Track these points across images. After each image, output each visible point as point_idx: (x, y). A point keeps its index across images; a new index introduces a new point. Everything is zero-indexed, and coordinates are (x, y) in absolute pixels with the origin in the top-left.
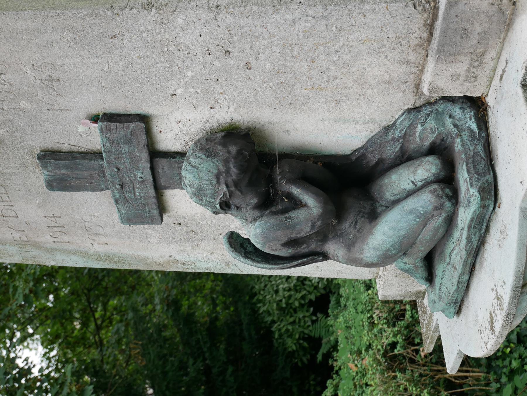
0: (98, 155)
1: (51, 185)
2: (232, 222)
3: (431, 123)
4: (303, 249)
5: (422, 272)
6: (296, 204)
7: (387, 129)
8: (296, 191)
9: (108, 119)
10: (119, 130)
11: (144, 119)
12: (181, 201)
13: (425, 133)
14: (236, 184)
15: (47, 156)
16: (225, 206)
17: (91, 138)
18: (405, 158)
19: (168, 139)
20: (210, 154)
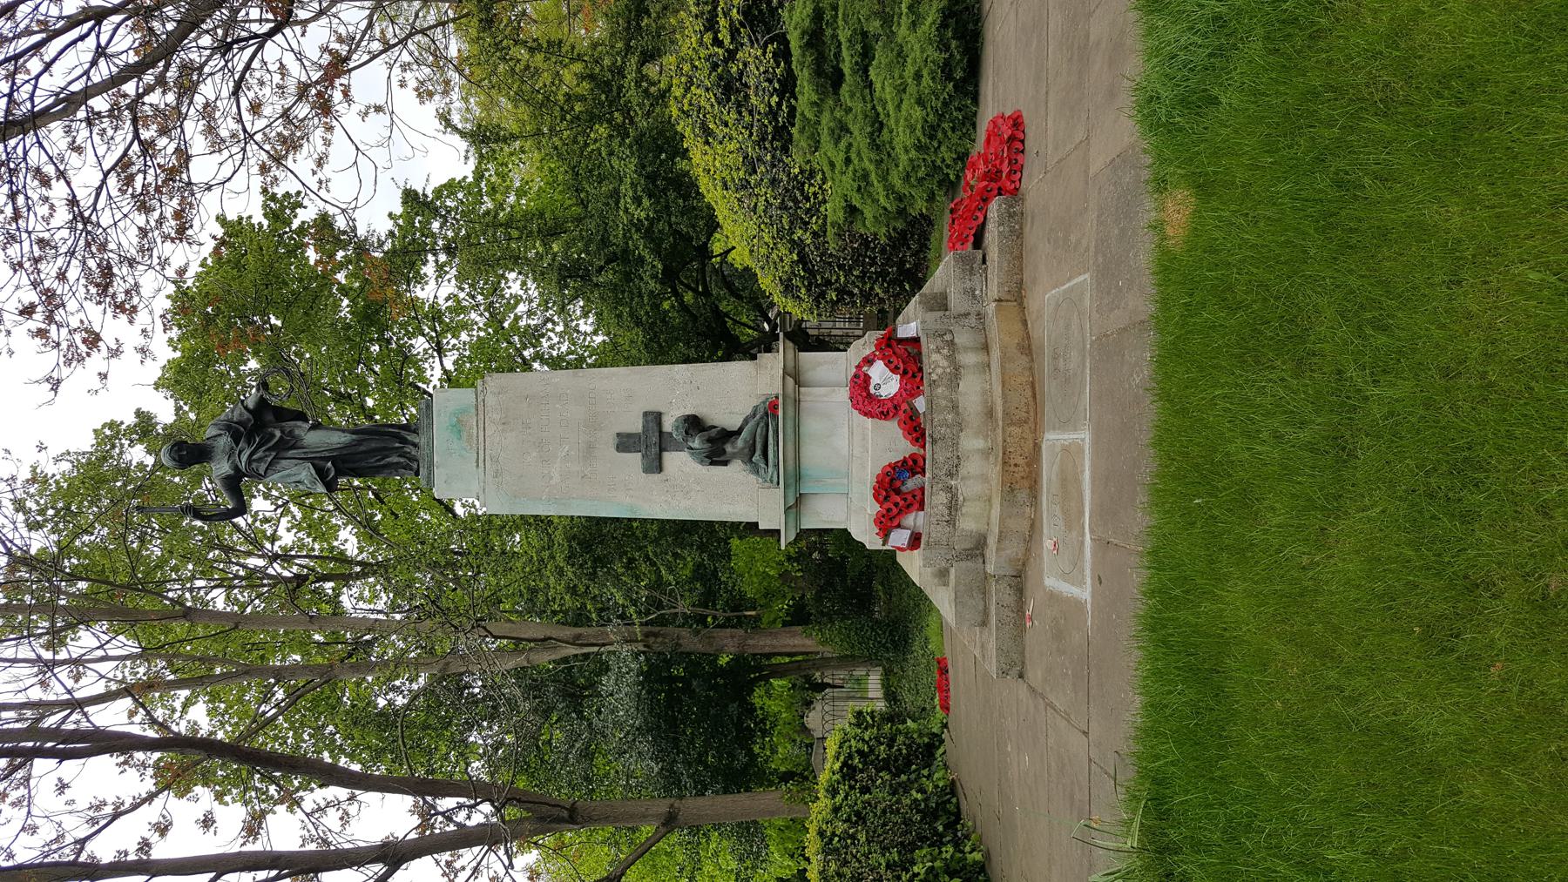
11: (660, 414)
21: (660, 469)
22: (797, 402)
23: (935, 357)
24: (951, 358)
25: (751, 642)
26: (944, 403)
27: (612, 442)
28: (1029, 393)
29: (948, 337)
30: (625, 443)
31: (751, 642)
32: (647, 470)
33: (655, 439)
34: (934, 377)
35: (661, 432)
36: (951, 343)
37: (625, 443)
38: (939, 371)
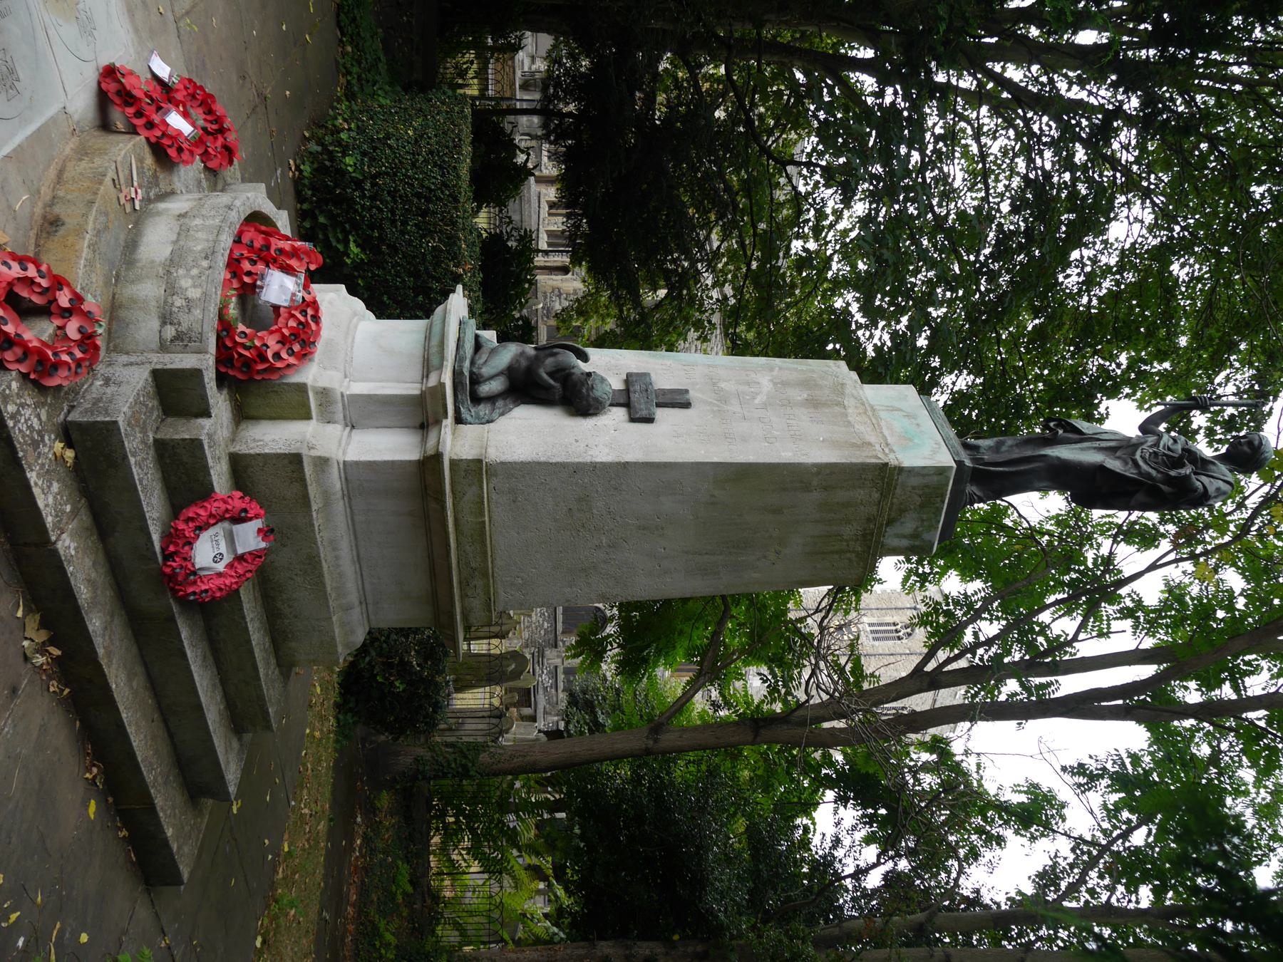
0: (659, 405)
1: (687, 391)
2: (584, 367)
3: (482, 414)
4: (547, 352)
5: (482, 340)
6: (550, 374)
7: (502, 414)
8: (552, 382)
9: (649, 420)
10: (644, 413)
11: (632, 420)
12: (616, 384)
13: (484, 409)
14: (583, 385)
15: (686, 405)
16: (589, 374)
17: (660, 413)
18: (492, 399)
19: (619, 414)
20: (596, 399)
21: (627, 382)
22: (426, 375)
23: (194, 293)
24: (172, 289)
25: (582, 952)
26: (200, 235)
27: (693, 395)
28: (66, 175)
29: (170, 332)
30: (677, 400)
31: (582, 952)
32: (646, 375)
33: (635, 397)
34: (205, 264)
35: (627, 405)
36: (166, 319)
37: (677, 400)
38: (195, 272)
